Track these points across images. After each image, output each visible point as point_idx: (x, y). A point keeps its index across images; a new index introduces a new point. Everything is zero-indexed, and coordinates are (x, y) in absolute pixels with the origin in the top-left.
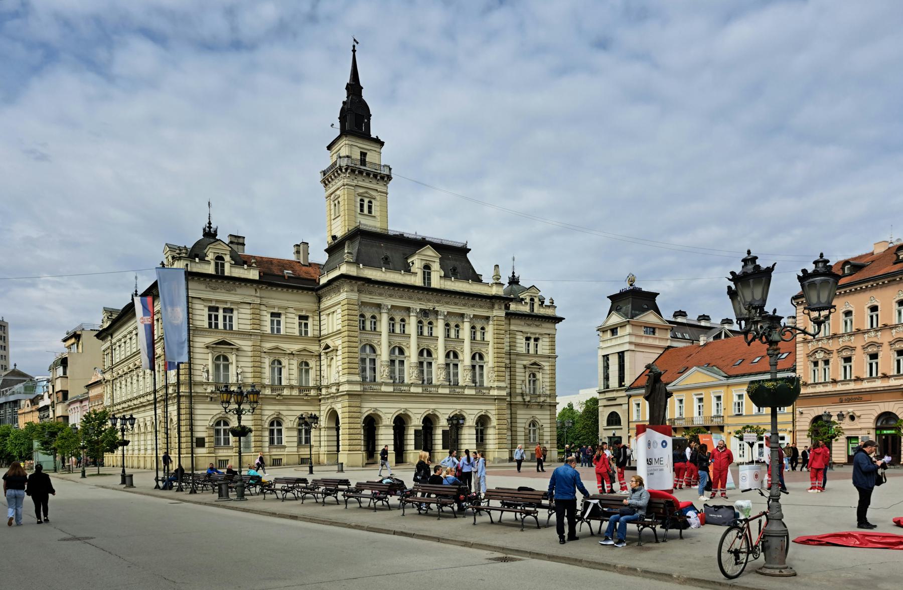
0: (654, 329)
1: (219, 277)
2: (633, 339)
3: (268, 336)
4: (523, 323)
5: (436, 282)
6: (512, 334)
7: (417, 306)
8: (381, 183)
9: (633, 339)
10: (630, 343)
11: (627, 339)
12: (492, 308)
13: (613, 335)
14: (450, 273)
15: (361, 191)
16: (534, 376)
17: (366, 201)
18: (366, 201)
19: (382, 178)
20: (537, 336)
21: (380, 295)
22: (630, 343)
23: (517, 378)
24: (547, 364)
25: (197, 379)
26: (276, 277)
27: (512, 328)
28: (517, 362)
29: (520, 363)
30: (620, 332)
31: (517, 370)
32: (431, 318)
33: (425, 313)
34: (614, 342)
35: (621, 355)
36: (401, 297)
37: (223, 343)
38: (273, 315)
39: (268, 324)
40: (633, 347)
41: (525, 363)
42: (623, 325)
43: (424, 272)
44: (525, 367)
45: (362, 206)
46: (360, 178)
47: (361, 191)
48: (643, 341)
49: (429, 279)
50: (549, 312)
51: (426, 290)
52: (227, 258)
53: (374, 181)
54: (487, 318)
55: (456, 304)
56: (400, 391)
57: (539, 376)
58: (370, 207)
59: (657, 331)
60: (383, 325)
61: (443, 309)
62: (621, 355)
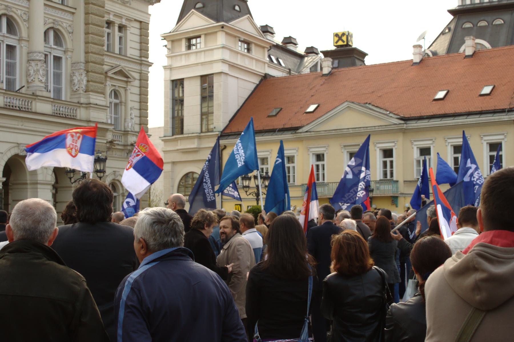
0: (248, 43)
2: (227, 56)
9: (227, 56)
10: (224, 61)
11: (218, 55)
13: (189, 47)
20: (124, 22)
22: (224, 61)
30: (200, 44)
34: (193, 60)
35: (206, 81)
40: (225, 68)
42: (209, 33)
48: (239, 61)
59: (253, 47)
62: (206, 81)
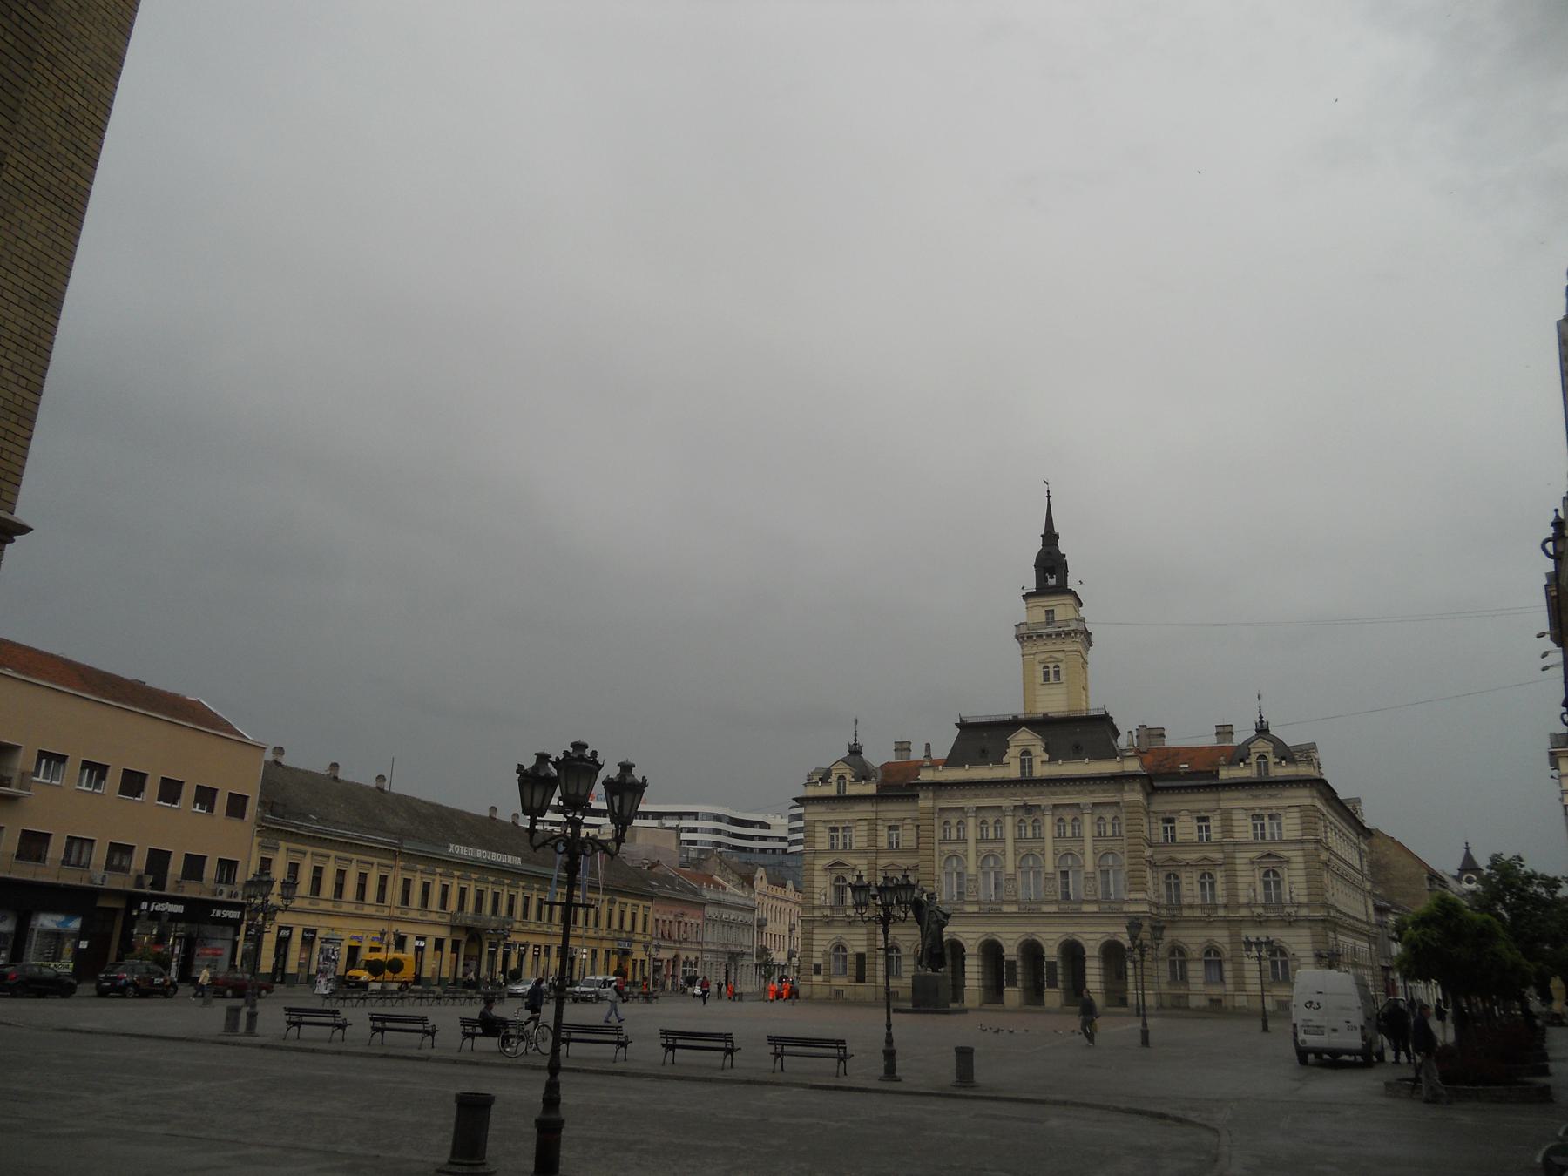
1: (842, 799)
3: (883, 851)
4: (1243, 795)
5: (1040, 771)
6: (1227, 814)
7: (1007, 802)
8: (1068, 641)
12: (1121, 791)
14: (1053, 755)
15: (1043, 656)
16: (1276, 874)
17: (1051, 666)
18: (1051, 666)
19: (1068, 634)
21: (964, 796)
23: (1239, 880)
24: (1300, 853)
25: (816, 902)
26: (898, 785)
27: (1223, 805)
28: (1238, 855)
29: (1243, 858)
31: (1238, 867)
32: (1038, 814)
33: (1029, 809)
36: (989, 796)
37: (839, 863)
38: (890, 828)
39: (885, 839)
41: (1251, 855)
43: (1023, 761)
44: (1253, 863)
45: (1046, 674)
46: (1040, 643)
47: (1043, 656)
49: (1031, 767)
50: (1303, 770)
51: (1027, 782)
52: (848, 777)
53: (1059, 641)
54: (1117, 804)
55: (1066, 793)
56: (1069, 908)
57: (1285, 874)
58: (1057, 673)
60: (972, 831)
61: (1046, 800)
